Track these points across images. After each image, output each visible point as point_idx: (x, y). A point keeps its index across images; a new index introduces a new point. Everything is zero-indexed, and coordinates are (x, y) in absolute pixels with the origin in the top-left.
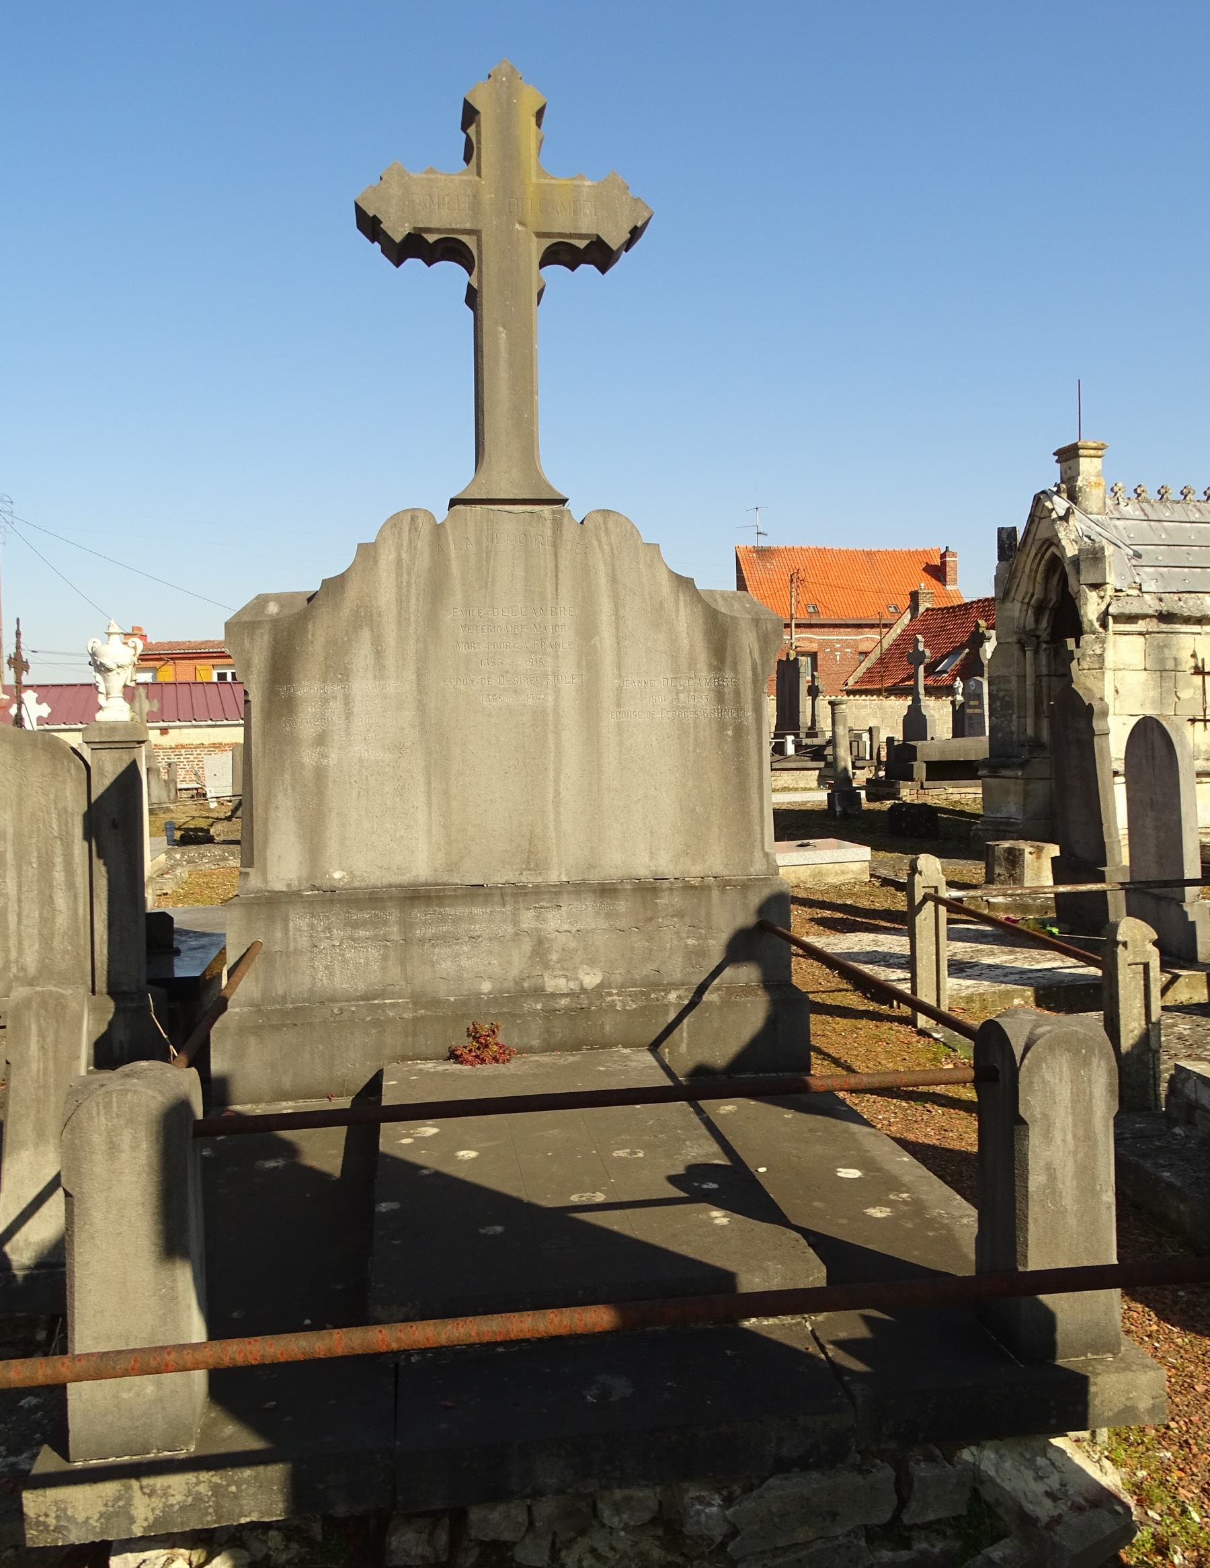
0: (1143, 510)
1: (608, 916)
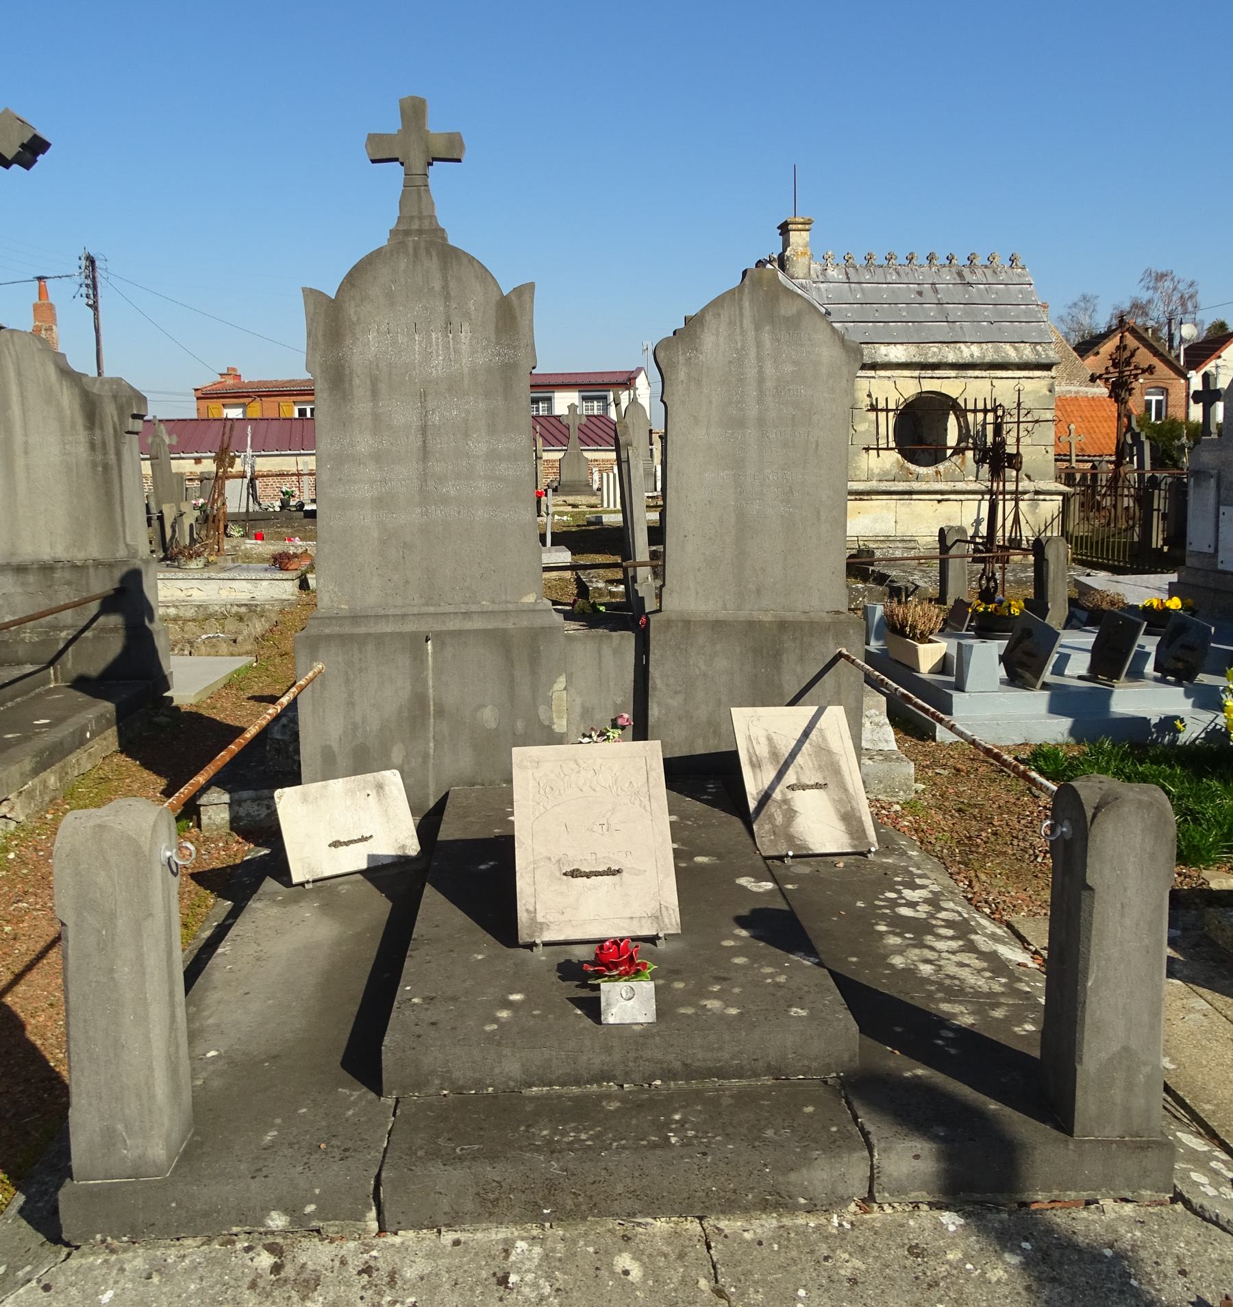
0: (847, 274)
1: (23, 584)
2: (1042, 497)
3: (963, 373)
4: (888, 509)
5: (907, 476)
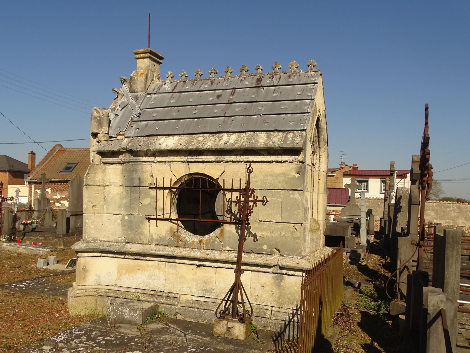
2: (284, 272)
3: (221, 158)
4: (160, 269)
5: (177, 241)
